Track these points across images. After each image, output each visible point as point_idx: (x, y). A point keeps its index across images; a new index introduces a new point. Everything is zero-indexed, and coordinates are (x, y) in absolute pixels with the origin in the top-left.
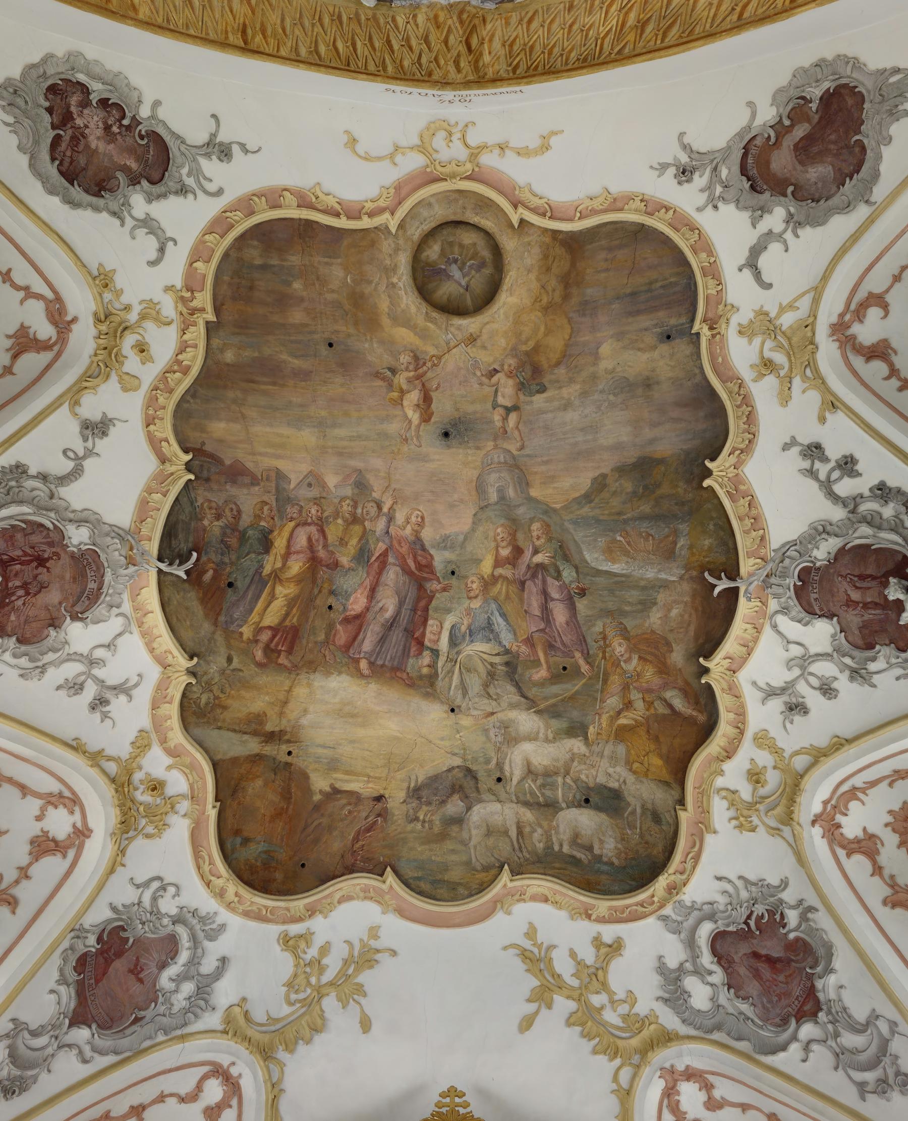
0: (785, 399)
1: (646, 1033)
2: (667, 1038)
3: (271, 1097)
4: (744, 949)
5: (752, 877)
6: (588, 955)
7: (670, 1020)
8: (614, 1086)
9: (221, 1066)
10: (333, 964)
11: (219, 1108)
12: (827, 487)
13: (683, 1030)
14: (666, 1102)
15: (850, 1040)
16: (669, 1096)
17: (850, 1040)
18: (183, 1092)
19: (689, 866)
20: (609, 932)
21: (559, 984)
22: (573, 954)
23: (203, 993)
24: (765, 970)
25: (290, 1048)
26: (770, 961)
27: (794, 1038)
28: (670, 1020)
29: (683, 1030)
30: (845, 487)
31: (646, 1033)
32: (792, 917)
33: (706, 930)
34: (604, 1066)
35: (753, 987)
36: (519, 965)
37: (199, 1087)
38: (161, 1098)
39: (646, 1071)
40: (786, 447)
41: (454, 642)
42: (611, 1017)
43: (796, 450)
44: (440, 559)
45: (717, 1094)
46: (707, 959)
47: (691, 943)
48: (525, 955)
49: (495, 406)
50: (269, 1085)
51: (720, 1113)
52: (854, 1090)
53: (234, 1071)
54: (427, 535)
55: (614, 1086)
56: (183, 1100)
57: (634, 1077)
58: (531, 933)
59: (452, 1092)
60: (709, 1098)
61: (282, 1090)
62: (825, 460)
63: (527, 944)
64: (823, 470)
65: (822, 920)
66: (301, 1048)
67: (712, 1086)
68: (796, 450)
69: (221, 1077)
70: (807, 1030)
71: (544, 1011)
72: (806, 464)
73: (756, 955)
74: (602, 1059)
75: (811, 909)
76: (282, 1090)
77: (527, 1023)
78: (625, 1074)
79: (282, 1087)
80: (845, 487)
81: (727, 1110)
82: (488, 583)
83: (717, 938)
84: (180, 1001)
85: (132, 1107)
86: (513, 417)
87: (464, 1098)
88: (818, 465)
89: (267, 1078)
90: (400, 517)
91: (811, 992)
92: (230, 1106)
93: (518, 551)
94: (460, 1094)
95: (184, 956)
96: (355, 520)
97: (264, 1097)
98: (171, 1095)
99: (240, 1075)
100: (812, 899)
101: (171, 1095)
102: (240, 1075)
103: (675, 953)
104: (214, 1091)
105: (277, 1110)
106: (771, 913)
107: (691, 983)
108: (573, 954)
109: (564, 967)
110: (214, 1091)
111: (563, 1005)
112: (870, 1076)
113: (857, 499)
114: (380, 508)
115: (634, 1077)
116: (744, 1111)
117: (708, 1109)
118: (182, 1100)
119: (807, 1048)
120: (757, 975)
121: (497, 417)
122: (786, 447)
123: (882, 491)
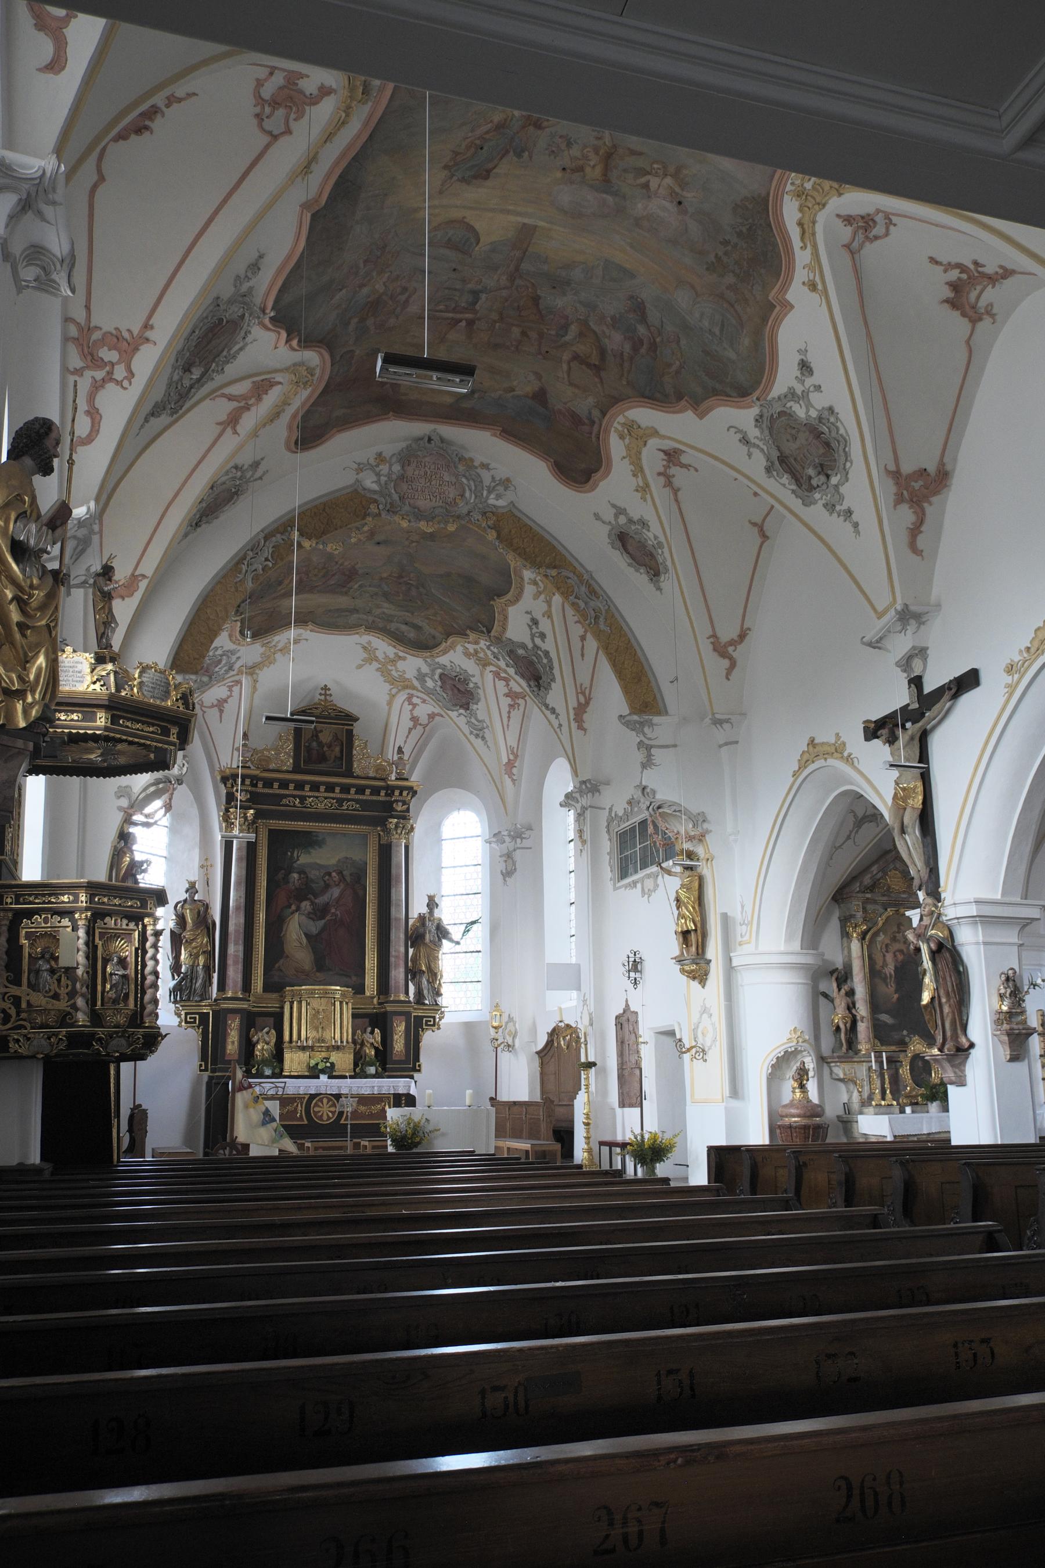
0: (536, 597)
1: (406, 683)
2: (414, 688)
4: (451, 682)
5: (463, 667)
6: (392, 656)
7: (416, 683)
10: (280, 646)
12: (533, 636)
13: (420, 688)
15: (473, 720)
17: (473, 720)
19: (441, 653)
20: (401, 654)
21: (376, 659)
22: (385, 653)
23: (231, 668)
24: (456, 691)
25: (260, 669)
26: (459, 690)
27: (457, 710)
28: (416, 683)
29: (420, 688)
30: (538, 641)
31: (406, 683)
32: (471, 685)
33: (439, 671)
34: (387, 686)
35: (450, 693)
36: (362, 650)
39: (402, 693)
40: (527, 612)
41: (361, 586)
42: (394, 673)
43: (529, 616)
44: (360, 572)
46: (437, 677)
47: (433, 671)
48: (365, 648)
49: (407, 539)
54: (357, 567)
57: (397, 693)
58: (369, 643)
62: (538, 628)
63: (366, 645)
64: (535, 630)
65: (480, 691)
66: (265, 668)
68: (530, 616)
70: (462, 711)
71: (368, 665)
72: (531, 624)
73: (454, 686)
74: (387, 684)
75: (478, 687)
77: (360, 667)
78: (394, 691)
80: (538, 641)
82: (382, 579)
83: (441, 676)
84: (222, 671)
86: (414, 544)
88: (534, 627)
90: (346, 563)
91: (468, 704)
93: (400, 577)
95: (224, 662)
96: (324, 568)
100: (480, 685)
103: (425, 669)
106: (465, 680)
107: (427, 679)
108: (385, 653)
109: (380, 655)
111: (376, 665)
113: (538, 648)
114: (337, 563)
115: (397, 693)
119: (460, 714)
120: (452, 690)
121: (407, 543)
122: (527, 612)
123: (547, 653)
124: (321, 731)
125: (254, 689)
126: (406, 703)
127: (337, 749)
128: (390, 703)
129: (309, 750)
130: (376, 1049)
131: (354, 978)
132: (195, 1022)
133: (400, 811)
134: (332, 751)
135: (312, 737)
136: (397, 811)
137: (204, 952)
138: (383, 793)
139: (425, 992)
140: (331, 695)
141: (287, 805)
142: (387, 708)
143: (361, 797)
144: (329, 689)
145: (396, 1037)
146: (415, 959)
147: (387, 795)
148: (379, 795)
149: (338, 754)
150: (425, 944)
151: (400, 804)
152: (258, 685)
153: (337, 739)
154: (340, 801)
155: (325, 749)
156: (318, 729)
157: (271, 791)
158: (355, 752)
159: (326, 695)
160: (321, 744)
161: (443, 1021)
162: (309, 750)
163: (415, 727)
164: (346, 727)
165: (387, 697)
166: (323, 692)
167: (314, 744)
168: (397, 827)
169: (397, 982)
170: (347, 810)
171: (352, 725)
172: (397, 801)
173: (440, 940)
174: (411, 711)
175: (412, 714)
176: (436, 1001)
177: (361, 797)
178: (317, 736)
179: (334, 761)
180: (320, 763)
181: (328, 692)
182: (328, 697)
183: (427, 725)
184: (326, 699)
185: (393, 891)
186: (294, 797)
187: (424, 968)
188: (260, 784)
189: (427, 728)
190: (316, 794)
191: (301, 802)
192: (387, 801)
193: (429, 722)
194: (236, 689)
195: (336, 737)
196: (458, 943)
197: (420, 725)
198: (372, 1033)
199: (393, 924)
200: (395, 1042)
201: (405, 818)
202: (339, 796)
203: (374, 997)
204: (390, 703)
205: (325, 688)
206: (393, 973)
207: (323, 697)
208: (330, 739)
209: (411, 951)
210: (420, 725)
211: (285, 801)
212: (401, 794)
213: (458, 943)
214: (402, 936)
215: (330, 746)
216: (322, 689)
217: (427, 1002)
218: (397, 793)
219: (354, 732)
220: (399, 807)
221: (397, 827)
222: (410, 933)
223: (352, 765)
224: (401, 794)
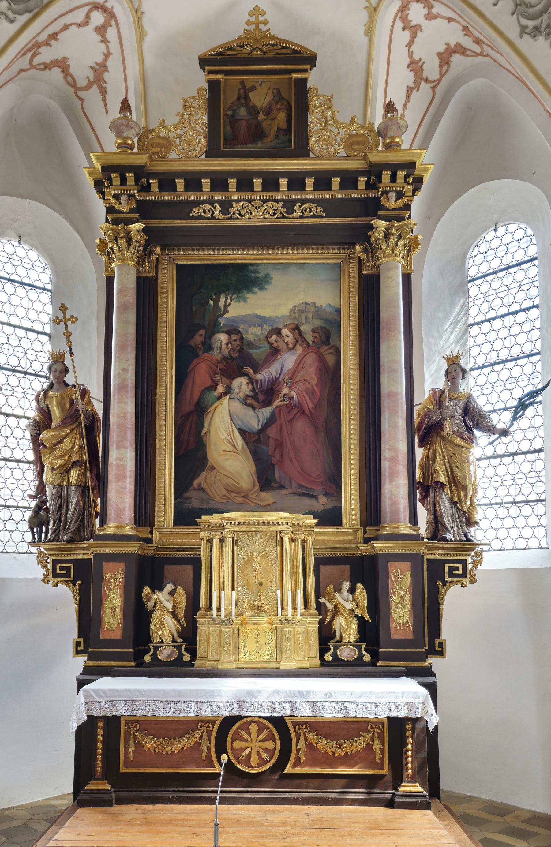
3: (136, 19)
8: (367, 4)
9: (99, 4)
11: (104, 27)
14: (399, 14)
16: (402, 11)
18: (78, 21)
37: (88, 17)
38: (66, 27)
45: (434, 11)
50: (134, 11)
51: (434, 22)
52: (518, 30)
53: (108, 5)
55: (367, 4)
56: (79, 25)
59: (257, 11)
60: (429, 13)
61: (142, 13)
67: (432, 7)
69: (100, 10)
76: (142, 13)
79: (142, 10)
81: (439, 20)
85: (49, 35)
87: (265, 17)
89: (131, 6)
92: (111, 26)
94: (262, 13)
97: (131, 19)
98: (72, 24)
99: (113, 7)
101: (72, 24)
102: (113, 7)
104: (98, 18)
105: (142, 26)
110: (98, 18)
112: (531, 24)
116: (449, 22)
117: (427, 19)
118: (79, 25)
124: (253, 88)
125: (141, 35)
126: (399, 25)
127: (281, 116)
128: (369, 31)
129: (233, 121)
130: (361, 620)
131: (323, 500)
132: (68, 575)
133: (393, 209)
134: (273, 119)
135: (239, 99)
136: (387, 209)
137: (75, 464)
138: (362, 182)
139: (447, 521)
140: (266, 23)
141: (201, 218)
142: (366, 39)
143: (324, 195)
144: (263, 13)
145: (395, 599)
146: (427, 468)
147: (370, 186)
148: (356, 188)
149: (284, 126)
150: (443, 438)
151: (393, 195)
152: (145, 21)
153: (281, 98)
154: (289, 205)
155: (261, 117)
156: (248, 86)
157: (173, 197)
158: (310, 118)
159: (258, 23)
160: (253, 111)
161: (480, 567)
162: (233, 121)
163: (417, 86)
164: (295, 75)
165: (364, 16)
166: (254, 18)
167: (243, 111)
168: (387, 236)
169: (395, 503)
170: (301, 217)
171: (305, 71)
172: (386, 193)
173: (469, 430)
174: (409, 45)
175: (410, 54)
176: (466, 535)
177: (324, 195)
178: (246, 98)
179: (277, 137)
180: (254, 142)
181: (261, 18)
182: (261, 26)
183: (439, 81)
184: (257, 28)
185: (383, 347)
186: (211, 202)
187: (443, 479)
188: (154, 184)
189: (437, 90)
190: (249, 196)
191: (224, 211)
192: (372, 199)
193: (442, 75)
194: (111, 33)
195: (278, 96)
196: (505, 433)
197: (426, 80)
198: (352, 590)
199: (385, 403)
200: (393, 608)
201: (400, 219)
202: (286, 197)
203: (356, 531)
204: (369, 31)
205: (257, 11)
206: (387, 488)
207: (253, 27)
208: (268, 99)
209: (420, 453)
210: (426, 80)
211: (196, 212)
212: (393, 179)
213: (505, 433)
214: (402, 424)
215: (268, 112)
216: (251, 14)
217: (449, 536)
218: (386, 175)
219: (310, 85)
220: (391, 202)
221: (387, 236)
222: (417, 420)
223: (306, 139)
224: (393, 179)
